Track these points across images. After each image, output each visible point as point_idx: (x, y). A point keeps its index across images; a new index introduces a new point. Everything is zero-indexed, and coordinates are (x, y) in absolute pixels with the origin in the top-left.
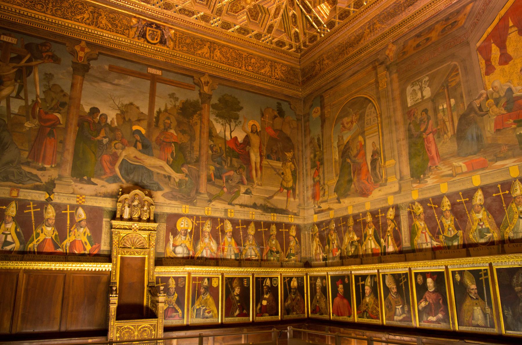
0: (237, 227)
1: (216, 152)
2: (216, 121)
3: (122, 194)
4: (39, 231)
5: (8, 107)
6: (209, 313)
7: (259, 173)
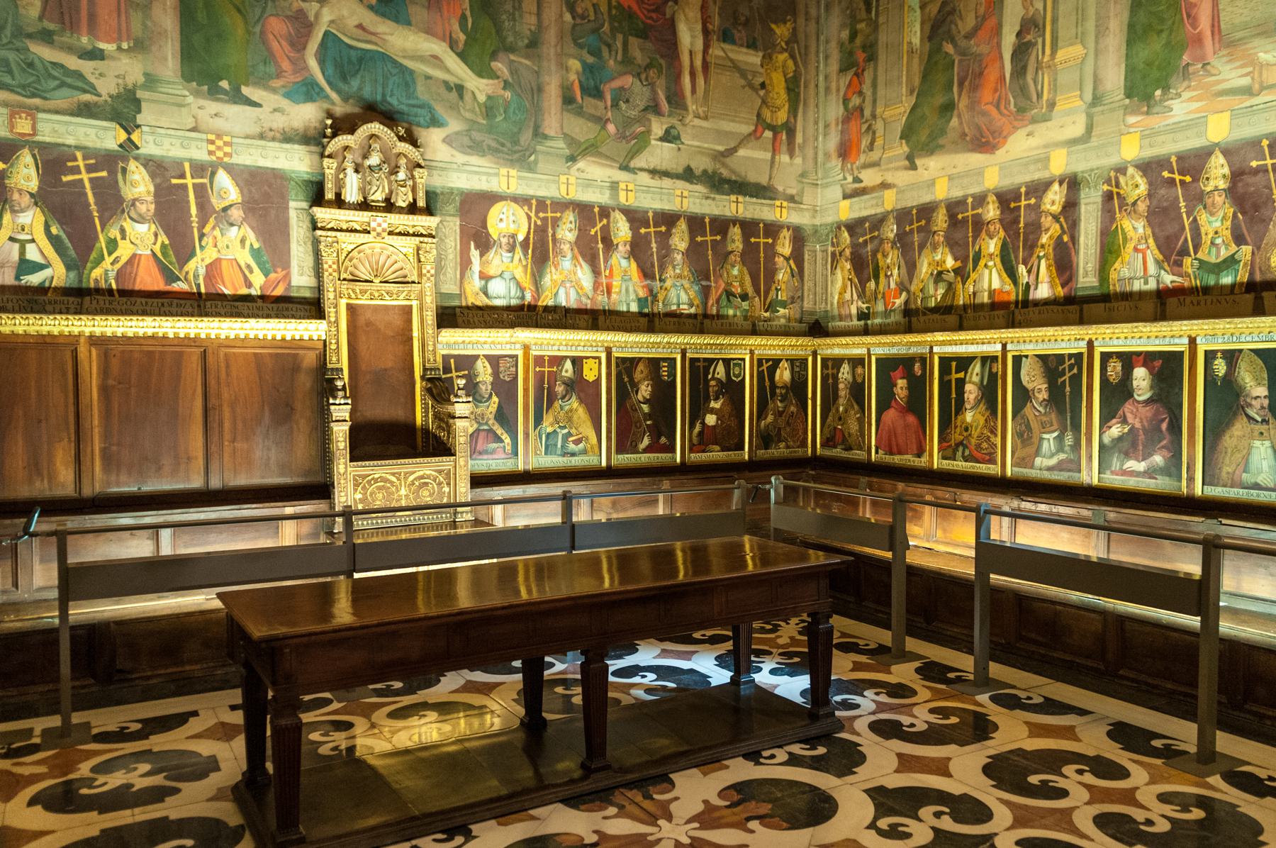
0: (643, 231)
1: (583, 17)
3: (334, 135)
4: (114, 233)
6: (577, 442)
7: (701, 81)
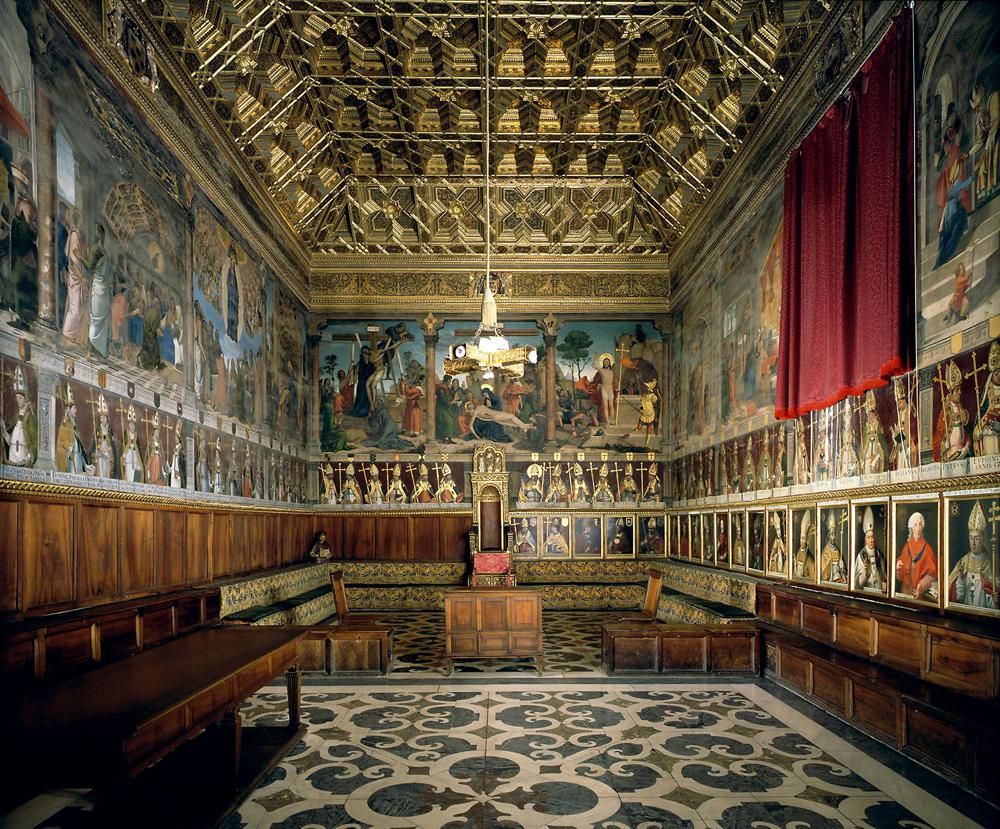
2: (563, 363)
5: (383, 388)
7: (613, 411)
